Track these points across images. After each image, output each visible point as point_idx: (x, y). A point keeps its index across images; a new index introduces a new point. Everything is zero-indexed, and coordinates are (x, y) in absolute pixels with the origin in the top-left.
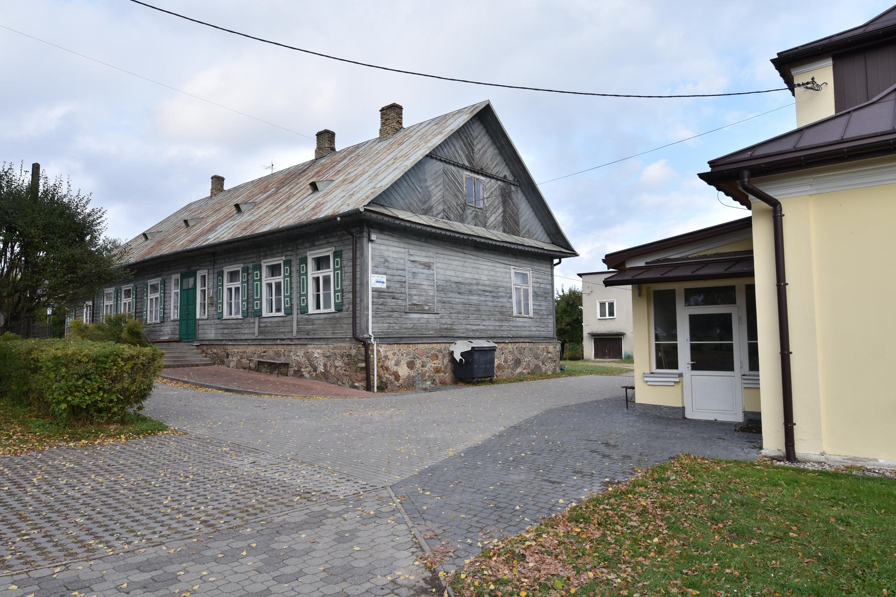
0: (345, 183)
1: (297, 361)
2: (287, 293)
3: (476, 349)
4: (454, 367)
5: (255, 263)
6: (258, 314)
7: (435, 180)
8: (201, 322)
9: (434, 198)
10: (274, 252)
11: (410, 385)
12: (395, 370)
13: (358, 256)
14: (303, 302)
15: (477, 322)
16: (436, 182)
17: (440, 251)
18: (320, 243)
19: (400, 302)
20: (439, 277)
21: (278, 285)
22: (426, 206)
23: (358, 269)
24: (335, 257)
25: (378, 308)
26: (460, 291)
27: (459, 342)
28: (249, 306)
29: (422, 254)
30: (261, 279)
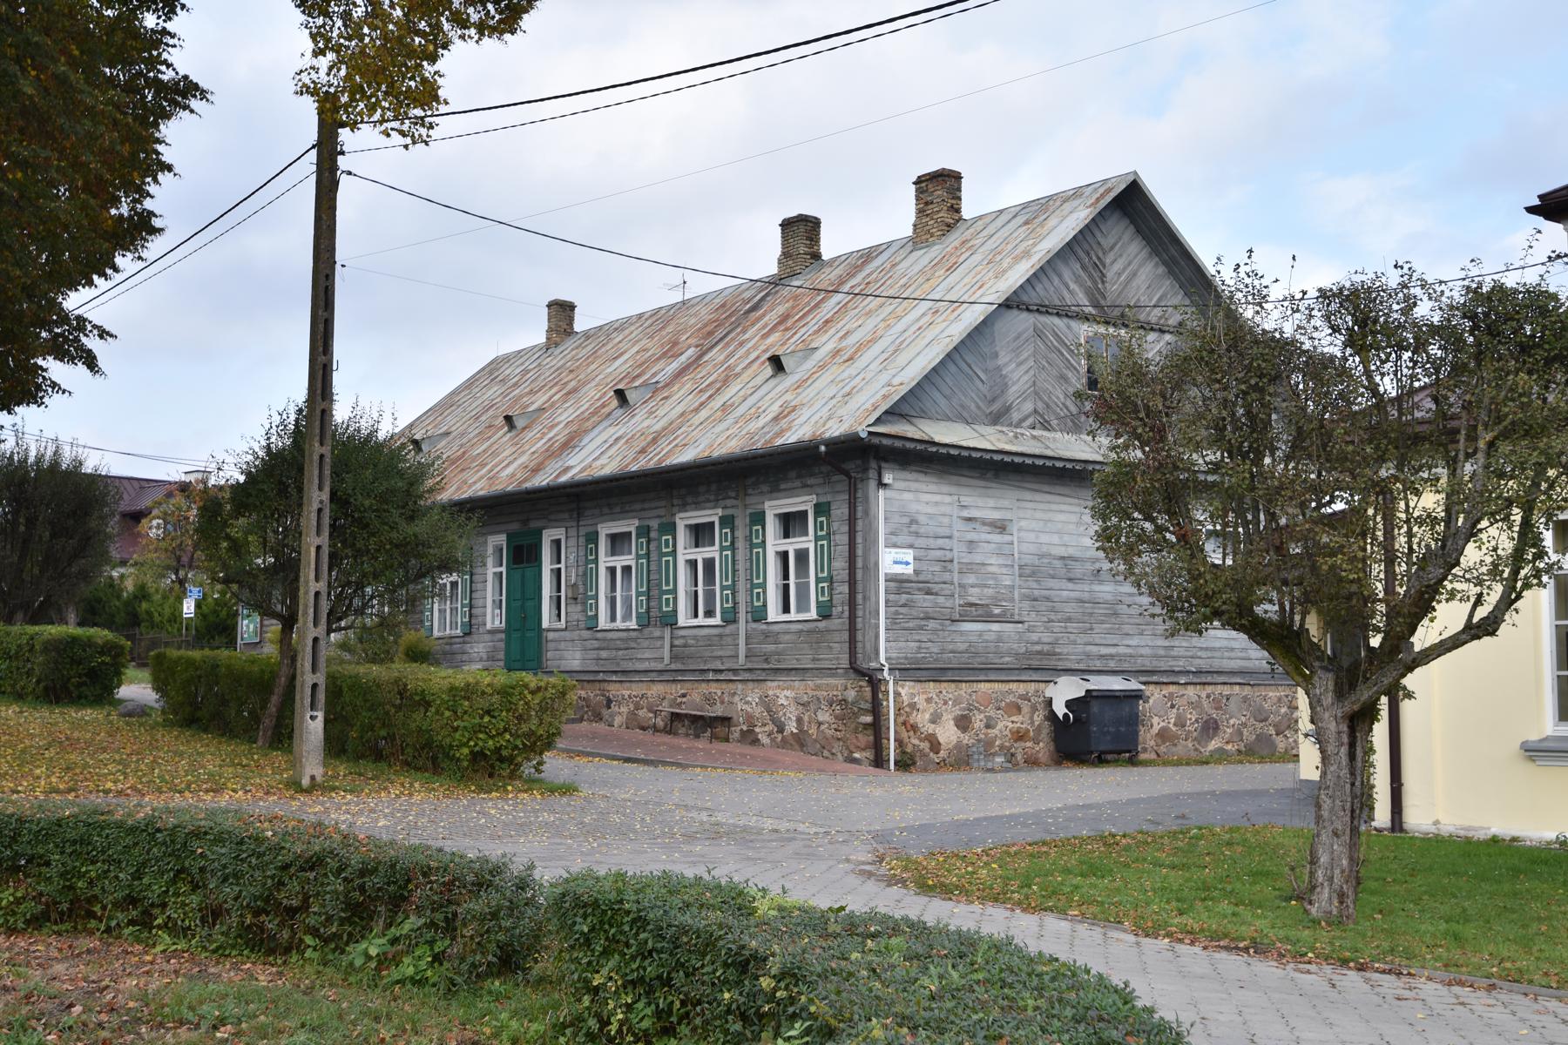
0: (838, 360)
1: (747, 713)
2: (727, 580)
3: (1094, 694)
4: (1055, 731)
5: (664, 520)
6: (670, 620)
7: (1017, 351)
8: (551, 635)
9: (1014, 388)
10: (701, 498)
11: (961, 761)
12: (930, 731)
13: (859, 514)
14: (758, 599)
16: (1017, 356)
17: (1028, 495)
18: (790, 485)
19: (941, 600)
20: (1025, 548)
21: (709, 564)
22: (996, 407)
23: (859, 540)
24: (817, 514)
25: (897, 613)
26: (1072, 576)
27: (1063, 680)
28: (652, 604)
29: (986, 502)
30: (675, 551)
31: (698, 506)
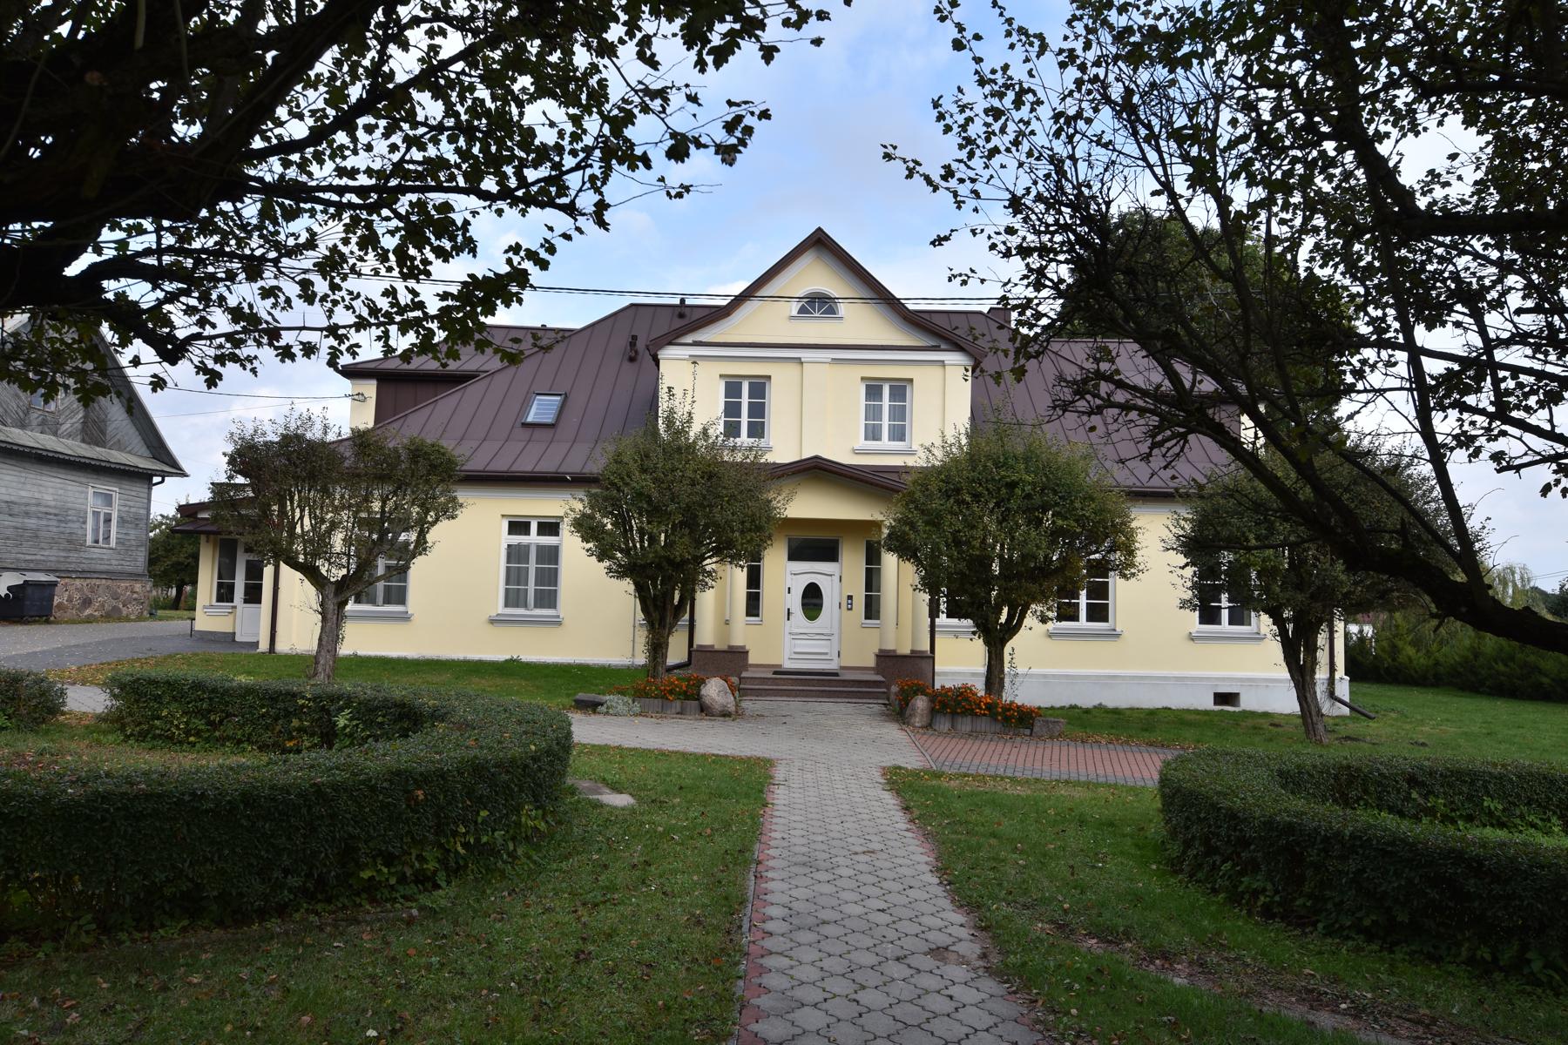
15: (33, 551)
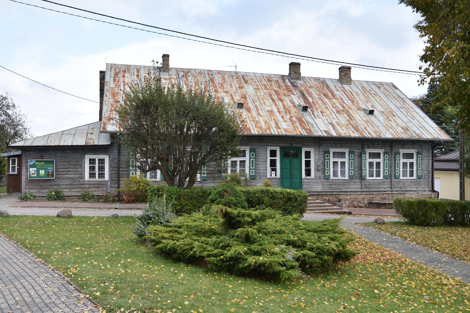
6: (362, 178)
10: (375, 146)
18: (408, 146)
31: (374, 148)
